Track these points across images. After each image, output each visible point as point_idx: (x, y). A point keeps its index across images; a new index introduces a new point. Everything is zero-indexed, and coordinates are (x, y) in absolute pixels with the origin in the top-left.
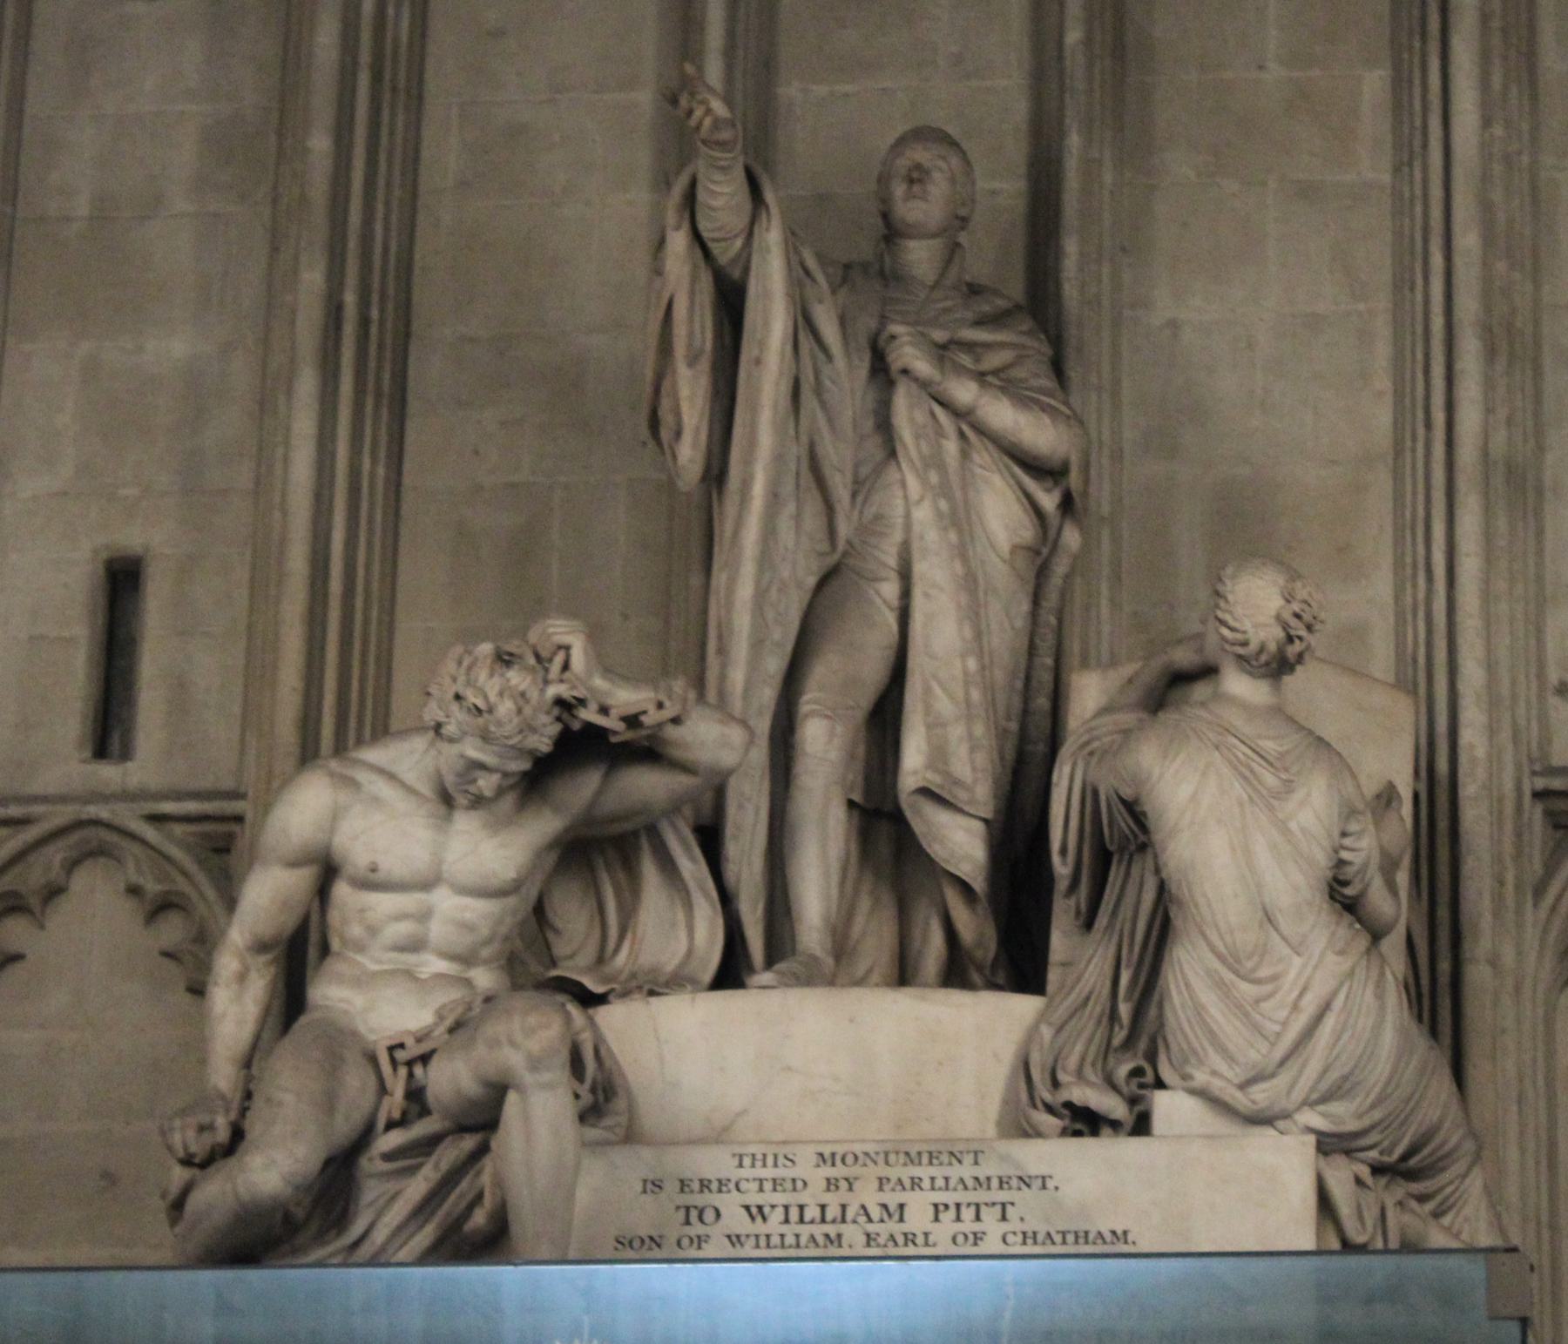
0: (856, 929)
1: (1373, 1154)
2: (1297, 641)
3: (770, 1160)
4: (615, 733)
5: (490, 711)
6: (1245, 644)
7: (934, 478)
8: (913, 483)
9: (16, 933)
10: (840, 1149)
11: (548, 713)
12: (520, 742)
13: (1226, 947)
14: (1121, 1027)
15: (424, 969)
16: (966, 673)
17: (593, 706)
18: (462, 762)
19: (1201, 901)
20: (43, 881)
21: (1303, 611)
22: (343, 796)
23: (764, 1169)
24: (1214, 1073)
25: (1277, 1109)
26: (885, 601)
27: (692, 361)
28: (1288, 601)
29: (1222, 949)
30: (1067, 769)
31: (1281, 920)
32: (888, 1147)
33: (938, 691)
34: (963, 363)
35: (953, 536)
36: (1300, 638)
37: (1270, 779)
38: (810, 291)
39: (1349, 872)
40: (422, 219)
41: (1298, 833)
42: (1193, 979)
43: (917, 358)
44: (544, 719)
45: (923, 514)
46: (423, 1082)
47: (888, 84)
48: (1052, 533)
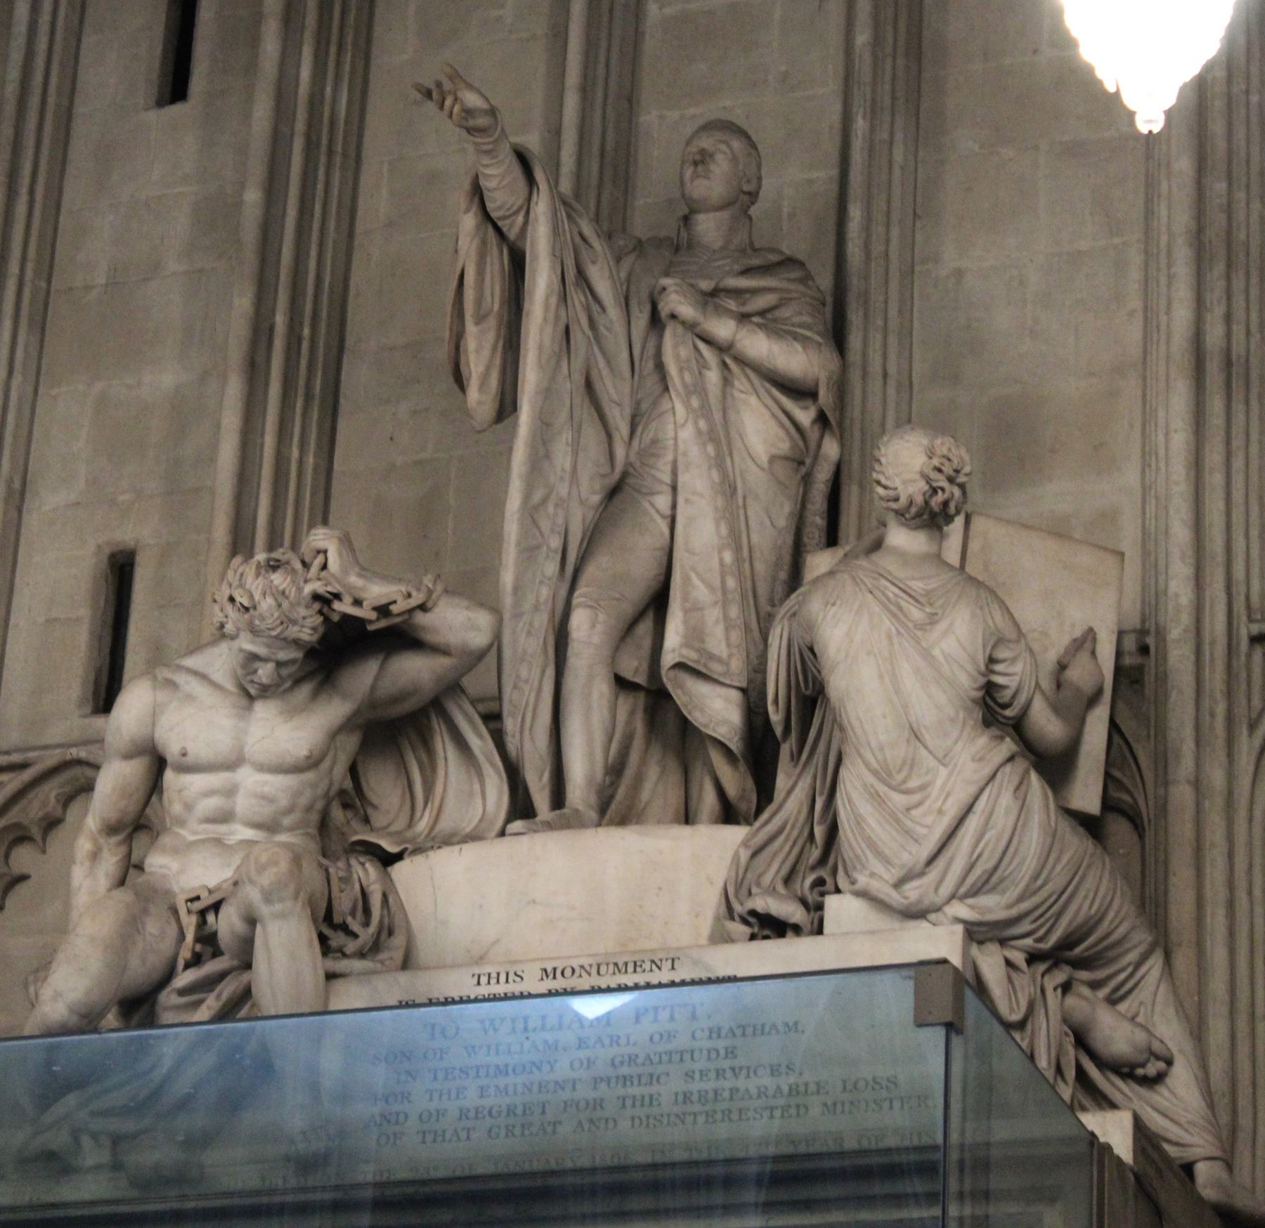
0: (645, 795)
1: (1029, 941)
2: (940, 492)
3: (503, 978)
4: (371, 622)
5: (255, 608)
6: (896, 499)
7: (695, 402)
8: (679, 408)
9: (23, 858)
10: (560, 965)
11: (307, 607)
12: (282, 632)
13: (877, 761)
14: (817, 847)
15: (231, 837)
16: (722, 564)
17: (348, 599)
18: (242, 655)
19: (855, 723)
20: (41, 814)
21: (942, 464)
22: (162, 696)
23: (498, 986)
24: (872, 875)
25: (926, 902)
26: (658, 511)
27: (479, 320)
28: (930, 458)
29: (876, 765)
30: (778, 631)
31: (927, 737)
32: (600, 960)
33: (696, 581)
34: (728, 306)
35: (710, 449)
36: (943, 490)
37: (916, 613)
38: (585, 254)
39: (1005, 696)
40: (357, 256)
41: (941, 658)
42: (854, 795)
43: (680, 303)
44: (302, 611)
45: (687, 434)
46: (214, 928)
47: (728, 103)
48: (813, 445)
